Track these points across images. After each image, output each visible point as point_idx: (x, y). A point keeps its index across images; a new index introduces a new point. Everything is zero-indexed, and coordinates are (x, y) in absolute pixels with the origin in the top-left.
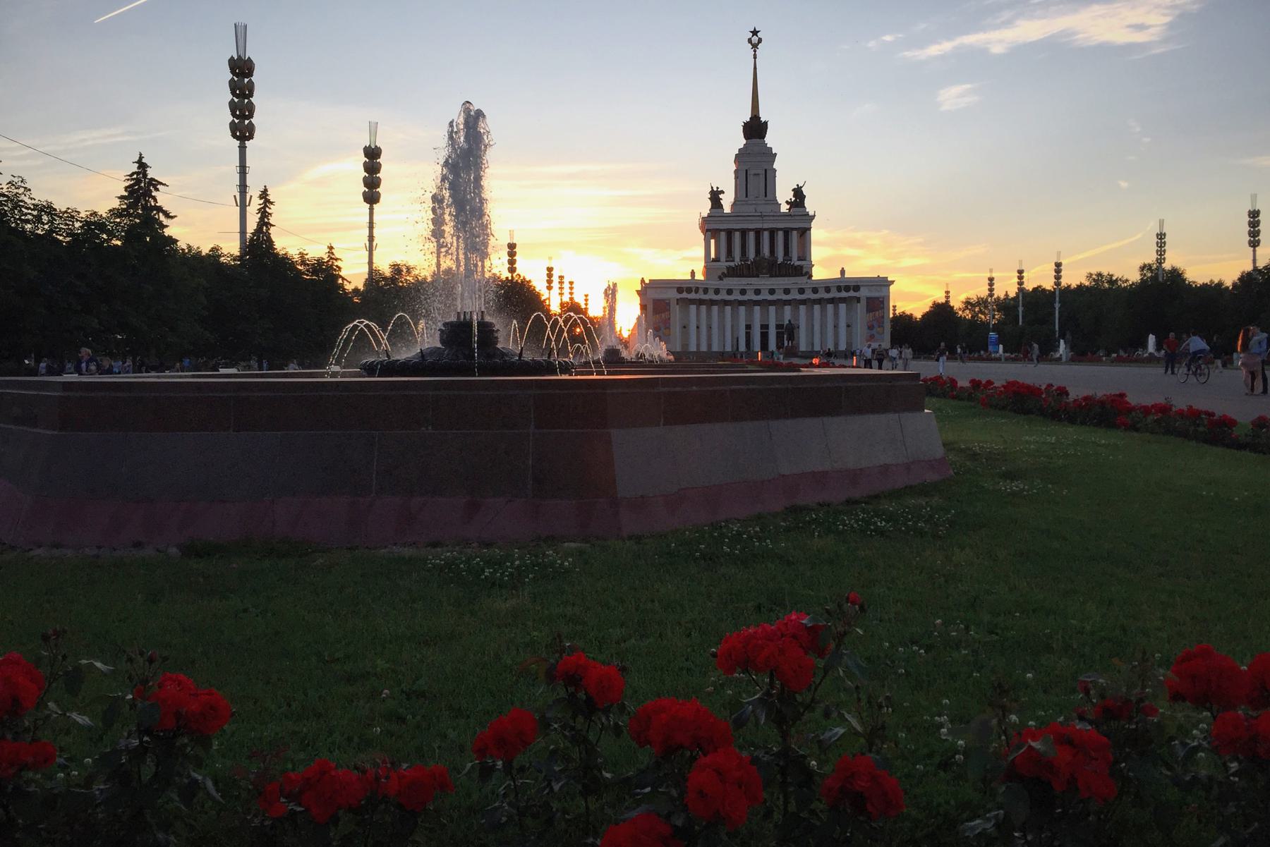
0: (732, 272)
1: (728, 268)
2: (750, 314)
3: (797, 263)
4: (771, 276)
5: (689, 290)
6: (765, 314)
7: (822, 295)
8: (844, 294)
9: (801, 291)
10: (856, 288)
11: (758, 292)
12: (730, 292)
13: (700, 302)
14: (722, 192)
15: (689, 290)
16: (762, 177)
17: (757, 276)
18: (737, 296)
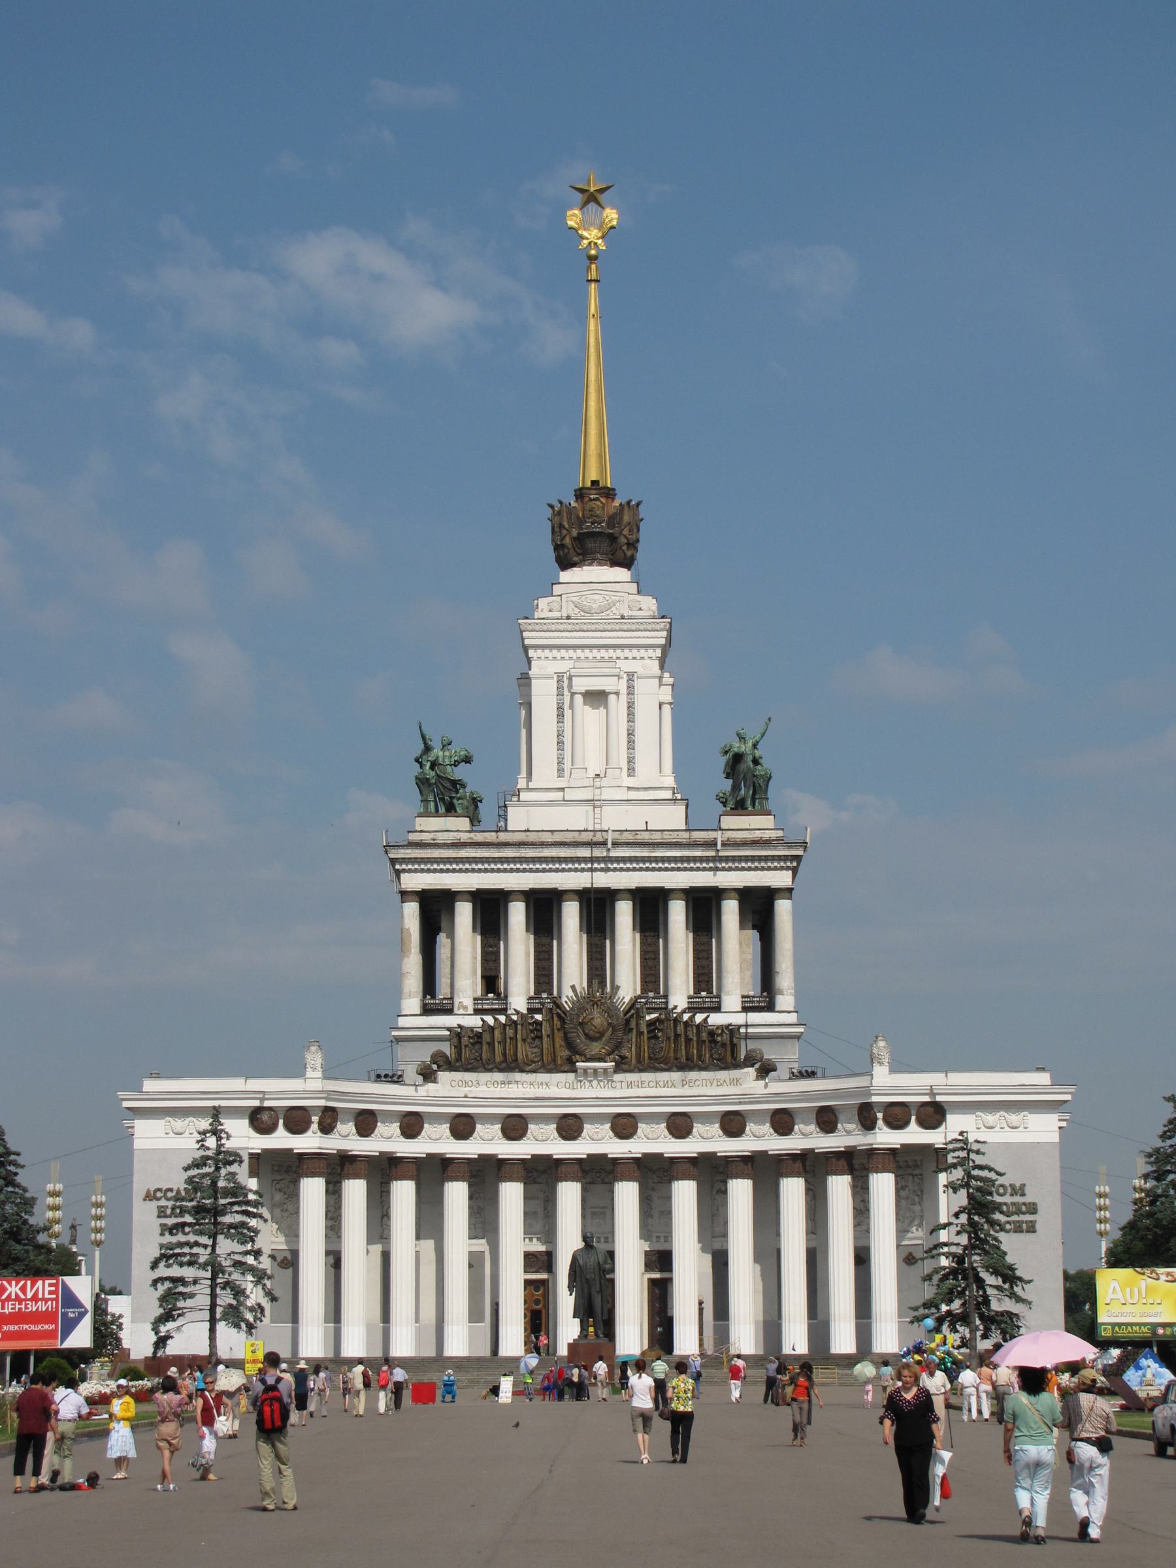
0: (470, 1053)
1: (458, 1035)
2: (541, 1215)
3: (738, 1019)
4: (622, 1066)
5: (297, 1120)
6: (598, 1212)
7: (807, 1138)
8: (885, 1137)
9: (733, 1124)
10: (933, 1114)
11: (570, 1127)
12: (462, 1127)
13: (337, 1168)
15: (297, 1120)
16: (618, 706)
17: (569, 1066)
18: (489, 1142)
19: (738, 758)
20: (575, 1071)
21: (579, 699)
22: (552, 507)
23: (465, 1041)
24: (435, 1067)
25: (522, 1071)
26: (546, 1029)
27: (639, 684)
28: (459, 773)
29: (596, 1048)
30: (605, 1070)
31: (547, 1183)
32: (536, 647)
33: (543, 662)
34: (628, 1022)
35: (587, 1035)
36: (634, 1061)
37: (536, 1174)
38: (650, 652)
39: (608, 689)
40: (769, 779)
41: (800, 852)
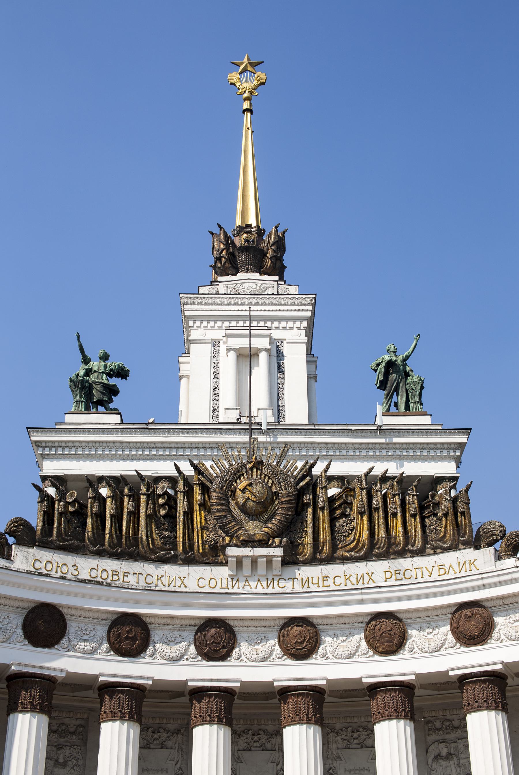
14: (122, 373)
17: (213, 555)
19: (390, 365)
20: (225, 563)
21: (232, 355)
22: (212, 234)
23: (59, 507)
24: (11, 540)
25: (145, 559)
26: (181, 507)
27: (286, 349)
28: (113, 381)
29: (254, 528)
30: (269, 560)
31: (180, 749)
32: (195, 319)
33: (201, 331)
34: (301, 493)
35: (243, 508)
36: (308, 551)
37: (164, 735)
38: (298, 324)
39: (259, 346)
40: (422, 388)
41: (464, 440)
